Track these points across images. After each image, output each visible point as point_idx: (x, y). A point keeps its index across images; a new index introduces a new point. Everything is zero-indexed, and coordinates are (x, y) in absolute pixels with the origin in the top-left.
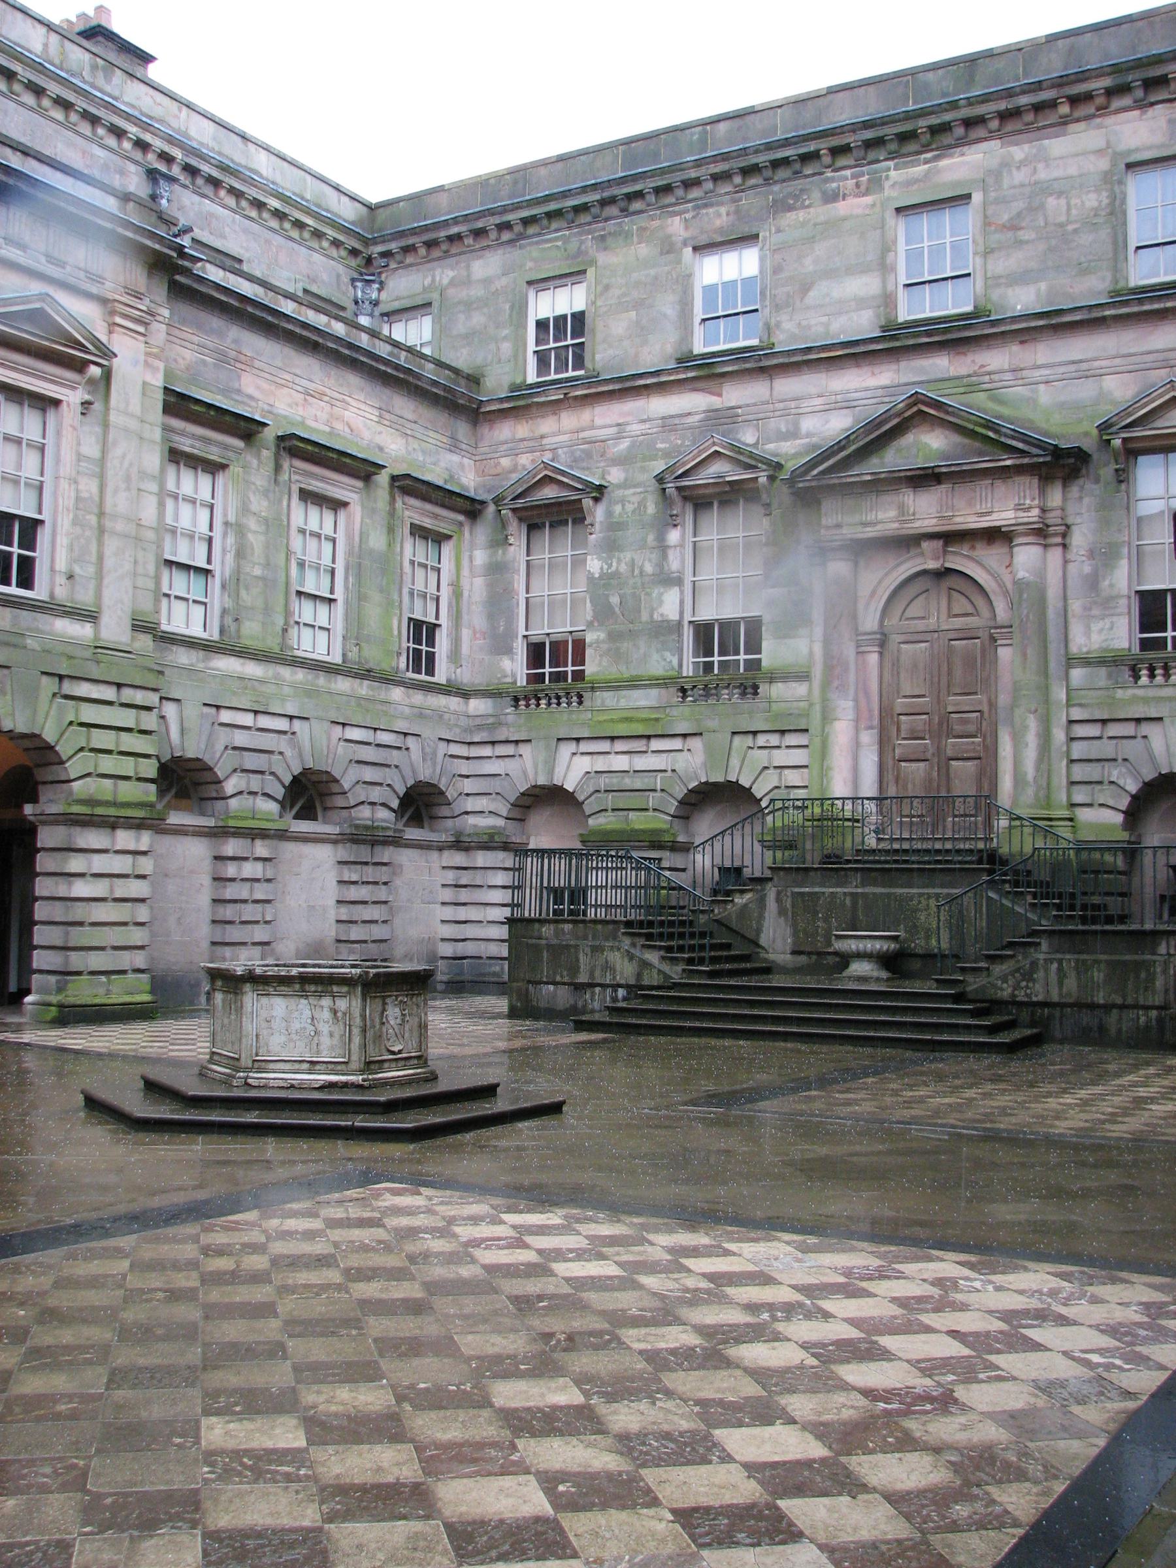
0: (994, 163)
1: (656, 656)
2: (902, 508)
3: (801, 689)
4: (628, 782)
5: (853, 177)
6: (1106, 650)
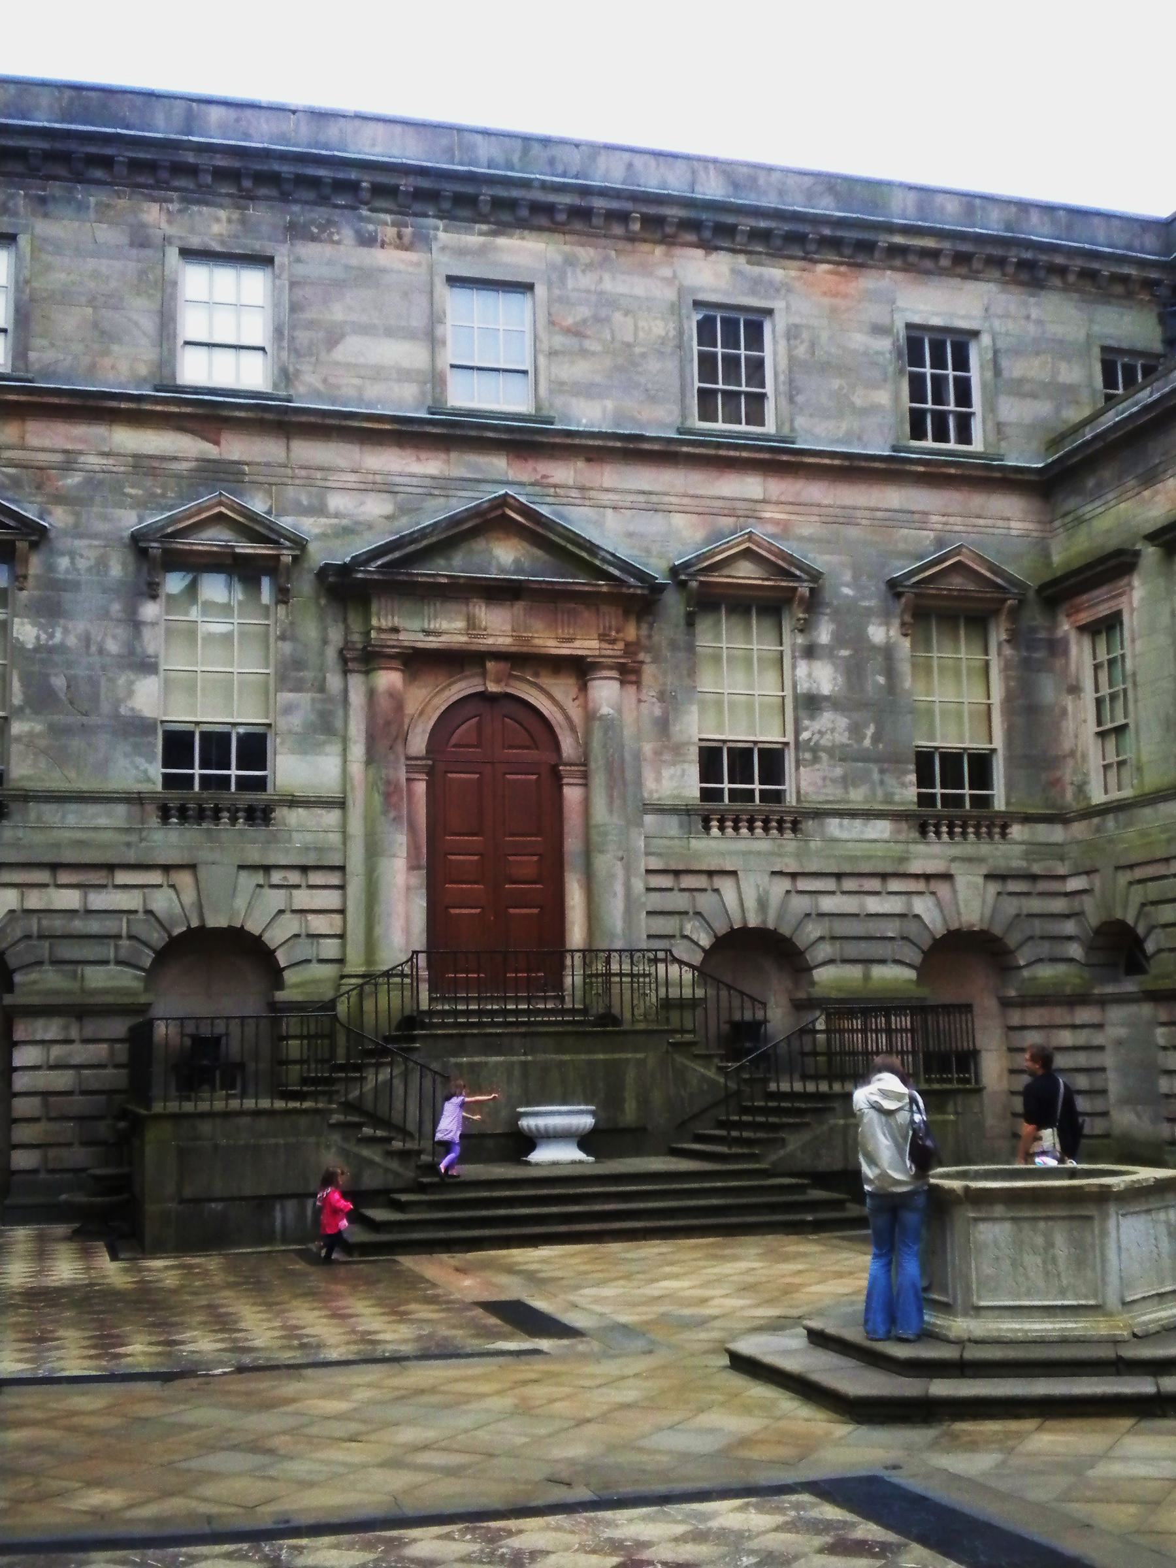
3: (331, 817)
4: (78, 925)
5: (394, 224)
6: (677, 797)
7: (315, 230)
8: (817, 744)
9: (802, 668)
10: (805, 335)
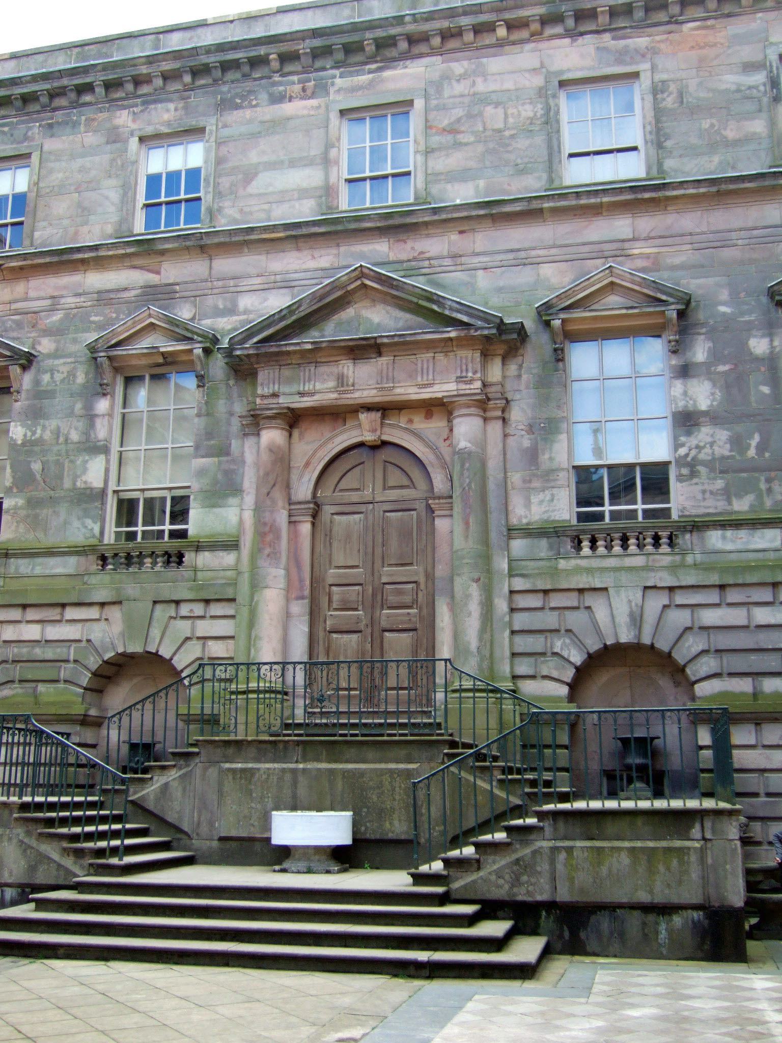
0: (436, 76)
1: (76, 523)
2: (341, 379)
3: (228, 558)
4: (38, 653)
5: (300, 82)
6: (547, 521)
7: (239, 101)
8: (693, 459)
9: (678, 387)
10: (673, 87)
